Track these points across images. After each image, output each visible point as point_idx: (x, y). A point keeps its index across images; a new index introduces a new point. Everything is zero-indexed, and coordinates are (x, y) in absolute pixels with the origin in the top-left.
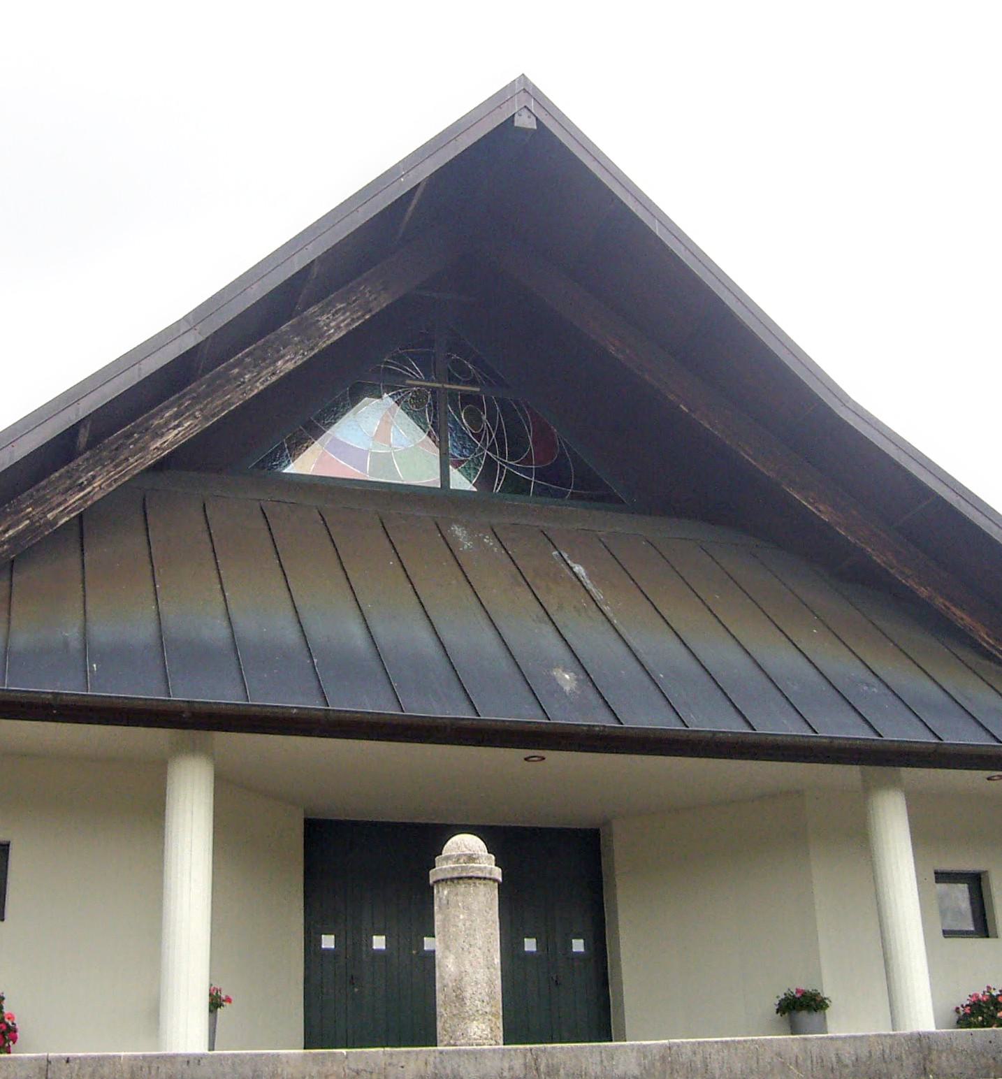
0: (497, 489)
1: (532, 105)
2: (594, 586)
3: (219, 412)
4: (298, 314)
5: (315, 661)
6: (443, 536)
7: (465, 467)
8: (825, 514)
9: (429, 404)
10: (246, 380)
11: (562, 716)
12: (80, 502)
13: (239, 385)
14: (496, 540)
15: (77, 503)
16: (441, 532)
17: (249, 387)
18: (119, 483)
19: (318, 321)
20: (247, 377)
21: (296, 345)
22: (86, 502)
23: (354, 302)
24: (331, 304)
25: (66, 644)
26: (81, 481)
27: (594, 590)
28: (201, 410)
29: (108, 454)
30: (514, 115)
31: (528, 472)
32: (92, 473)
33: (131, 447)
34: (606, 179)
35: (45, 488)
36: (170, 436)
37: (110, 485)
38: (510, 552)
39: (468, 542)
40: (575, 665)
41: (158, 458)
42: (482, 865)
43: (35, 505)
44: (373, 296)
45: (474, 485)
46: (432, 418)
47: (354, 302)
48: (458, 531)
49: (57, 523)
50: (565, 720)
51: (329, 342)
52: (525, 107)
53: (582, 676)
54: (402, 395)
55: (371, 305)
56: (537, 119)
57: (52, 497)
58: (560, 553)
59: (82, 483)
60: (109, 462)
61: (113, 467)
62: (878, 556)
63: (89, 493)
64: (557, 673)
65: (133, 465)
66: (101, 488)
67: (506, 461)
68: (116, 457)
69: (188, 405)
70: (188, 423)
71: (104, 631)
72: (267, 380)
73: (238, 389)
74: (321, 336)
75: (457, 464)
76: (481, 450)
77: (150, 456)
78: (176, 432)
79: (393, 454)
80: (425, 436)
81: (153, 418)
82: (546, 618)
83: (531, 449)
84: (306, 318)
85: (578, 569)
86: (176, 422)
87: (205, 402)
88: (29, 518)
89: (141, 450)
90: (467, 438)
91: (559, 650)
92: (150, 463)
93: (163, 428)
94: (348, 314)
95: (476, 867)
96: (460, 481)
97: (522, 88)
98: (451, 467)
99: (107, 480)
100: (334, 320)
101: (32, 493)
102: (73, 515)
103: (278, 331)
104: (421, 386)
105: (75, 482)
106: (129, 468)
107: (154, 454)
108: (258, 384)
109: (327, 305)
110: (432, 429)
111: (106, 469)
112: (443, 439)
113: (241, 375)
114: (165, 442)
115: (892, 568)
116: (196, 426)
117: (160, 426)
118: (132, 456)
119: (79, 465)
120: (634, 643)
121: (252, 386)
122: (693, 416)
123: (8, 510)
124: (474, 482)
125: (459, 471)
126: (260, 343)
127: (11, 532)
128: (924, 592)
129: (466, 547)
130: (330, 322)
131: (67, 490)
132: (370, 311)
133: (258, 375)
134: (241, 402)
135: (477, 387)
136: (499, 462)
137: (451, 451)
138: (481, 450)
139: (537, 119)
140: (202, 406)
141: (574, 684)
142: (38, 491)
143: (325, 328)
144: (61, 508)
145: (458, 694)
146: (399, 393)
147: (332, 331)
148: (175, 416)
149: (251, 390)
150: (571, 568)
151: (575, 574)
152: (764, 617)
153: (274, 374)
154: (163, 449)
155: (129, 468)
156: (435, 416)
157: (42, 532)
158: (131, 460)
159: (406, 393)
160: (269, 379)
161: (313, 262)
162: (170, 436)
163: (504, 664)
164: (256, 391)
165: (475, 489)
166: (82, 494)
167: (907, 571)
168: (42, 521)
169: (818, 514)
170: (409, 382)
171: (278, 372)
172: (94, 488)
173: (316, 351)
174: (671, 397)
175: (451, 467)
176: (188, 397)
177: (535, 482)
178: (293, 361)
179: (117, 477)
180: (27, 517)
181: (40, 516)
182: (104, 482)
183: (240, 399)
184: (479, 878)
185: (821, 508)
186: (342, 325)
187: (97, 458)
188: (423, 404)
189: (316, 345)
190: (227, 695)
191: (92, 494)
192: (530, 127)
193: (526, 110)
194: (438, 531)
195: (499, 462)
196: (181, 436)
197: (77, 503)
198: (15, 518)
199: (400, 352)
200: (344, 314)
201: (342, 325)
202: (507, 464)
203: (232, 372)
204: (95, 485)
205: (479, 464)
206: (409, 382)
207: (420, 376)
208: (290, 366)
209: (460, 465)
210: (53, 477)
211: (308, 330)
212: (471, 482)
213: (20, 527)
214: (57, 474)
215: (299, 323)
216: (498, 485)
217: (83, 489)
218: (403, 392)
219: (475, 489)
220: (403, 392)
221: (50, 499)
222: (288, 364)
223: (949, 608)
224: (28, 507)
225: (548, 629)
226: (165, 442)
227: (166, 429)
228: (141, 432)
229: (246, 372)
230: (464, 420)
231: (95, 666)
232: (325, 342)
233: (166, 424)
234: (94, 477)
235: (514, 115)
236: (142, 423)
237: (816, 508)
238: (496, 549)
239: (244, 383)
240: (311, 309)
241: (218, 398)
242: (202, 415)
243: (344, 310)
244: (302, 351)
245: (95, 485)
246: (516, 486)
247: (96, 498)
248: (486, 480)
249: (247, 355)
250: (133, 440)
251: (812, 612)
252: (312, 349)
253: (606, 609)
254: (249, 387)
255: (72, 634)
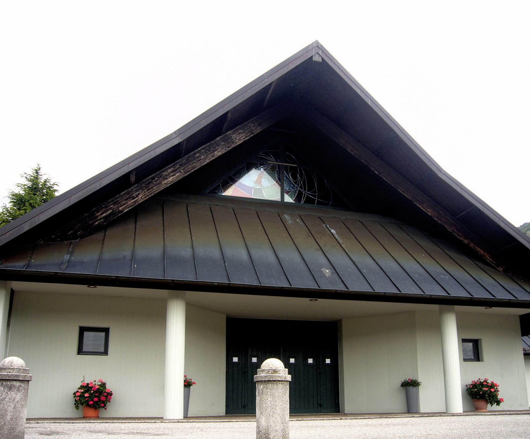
0: (302, 202)
1: (320, 52)
2: (339, 238)
3: (190, 171)
4: (223, 134)
5: (226, 264)
6: (281, 218)
7: (290, 194)
8: (429, 212)
9: (277, 171)
10: (202, 158)
11: (325, 286)
12: (133, 203)
13: (199, 160)
14: (301, 220)
15: (132, 204)
16: (280, 217)
17: (203, 161)
18: (149, 197)
19: (232, 137)
20: (202, 157)
21: (223, 146)
22: (135, 203)
23: (246, 130)
24: (237, 130)
25: (125, 257)
26: (133, 196)
27: (339, 239)
28: (183, 169)
29: (144, 185)
30: (312, 56)
31: (315, 196)
32: (137, 193)
33: (154, 183)
34: (349, 83)
35: (118, 198)
36: (171, 179)
37: (146, 197)
38: (306, 225)
39: (291, 221)
40: (330, 267)
41: (166, 187)
42: (281, 375)
43: (115, 204)
44: (254, 128)
45: (294, 200)
46: (278, 176)
47: (246, 130)
48: (287, 217)
49: (123, 212)
50: (326, 288)
51: (236, 145)
52: (317, 53)
53: (333, 271)
54: (267, 167)
55: (253, 131)
56: (322, 58)
57: (121, 202)
58: (326, 225)
59: (134, 196)
60: (145, 188)
61: (147, 190)
62: (449, 228)
63: (137, 200)
64: (323, 270)
65: (155, 190)
66: (142, 198)
67: (306, 192)
68: (148, 187)
69: (178, 167)
70: (178, 174)
71: (141, 253)
72: (210, 158)
73: (199, 162)
74: (233, 143)
75: (287, 193)
76: (297, 188)
77: (162, 187)
78: (173, 177)
79: (262, 189)
80: (275, 182)
81: (163, 172)
82: (320, 249)
83: (316, 189)
84: (227, 136)
85: (333, 231)
86: (173, 174)
87: (185, 166)
88: (111, 209)
89: (159, 184)
90: (291, 183)
91: (323, 260)
92: (162, 189)
93: (167, 176)
94: (244, 134)
95: (278, 376)
96: (288, 199)
97: (316, 45)
98: (285, 194)
99: (144, 195)
100: (239, 136)
101: (113, 200)
102: (130, 208)
103: (215, 140)
104: (274, 164)
105: (131, 195)
106: (153, 191)
107: (163, 186)
108: (207, 160)
109: (235, 131)
110: (278, 180)
111: (143, 191)
112: (282, 183)
113: (199, 157)
114: (168, 181)
115: (454, 233)
116: (181, 175)
117: (166, 175)
118: (155, 187)
119: (132, 189)
120: (354, 259)
121: (205, 160)
122: (380, 175)
123: (103, 206)
124: (294, 199)
125: (288, 195)
126: (208, 144)
127: (104, 215)
128: (466, 242)
129: (289, 223)
130: (237, 137)
131: (127, 199)
132: (253, 134)
133: (206, 157)
134: (200, 167)
135: (295, 164)
136: (303, 192)
137: (285, 188)
138: (297, 188)
139: (322, 58)
140: (184, 168)
141: (330, 274)
142: (115, 199)
143: (235, 140)
144: (125, 206)
145: (283, 277)
146: (265, 166)
147: (237, 141)
148: (173, 172)
149: (204, 162)
150: (330, 231)
151: (331, 233)
152: (405, 250)
153: (213, 156)
154: (167, 184)
155: (153, 191)
156: (279, 175)
157: (118, 215)
158: (154, 188)
159: (268, 166)
160: (211, 158)
161: (228, 111)
162: (171, 179)
163: (303, 266)
164: (206, 163)
165: (294, 202)
166: (134, 200)
167: (460, 234)
168: (117, 211)
169: (427, 212)
170: (269, 162)
171: (215, 155)
172: (139, 198)
173: (231, 148)
174: (372, 169)
175: (285, 194)
176: (178, 164)
177: (317, 200)
178: (221, 152)
179: (148, 194)
180: (111, 209)
181: (117, 209)
182: (143, 196)
183: (199, 166)
184: (279, 381)
185: (428, 210)
186: (241, 138)
187: (140, 187)
188: (275, 171)
189: (231, 146)
190: (189, 277)
191: (138, 200)
192: (319, 61)
193: (317, 54)
194: (279, 217)
195: (303, 192)
196: (175, 179)
197: (132, 204)
198: (106, 209)
199: (266, 151)
200: (242, 134)
201: (241, 138)
202: (306, 193)
203: (196, 155)
204: (139, 197)
205: (296, 193)
206: (269, 162)
207: (274, 160)
208: (220, 154)
209: (288, 193)
210: (121, 194)
211: (228, 140)
212: (292, 199)
213: (108, 213)
214: (123, 193)
215: (224, 137)
216: (303, 200)
217: (134, 198)
218: (267, 166)
219: (294, 202)
220: (267, 166)
221: (120, 202)
222: (219, 153)
223: (475, 248)
224: (111, 205)
225: (320, 253)
226: (168, 181)
227: (169, 176)
228: (158, 177)
229: (202, 155)
230: (290, 177)
231: (135, 265)
232: (234, 145)
233: (169, 174)
234: (139, 194)
235: (312, 56)
236: (158, 174)
237: (426, 210)
238: (301, 224)
239: (201, 159)
240: (228, 132)
241: (190, 165)
242: (184, 171)
243: (243, 133)
244: (225, 148)
245: (139, 197)
246: (309, 201)
247: (140, 202)
248: (298, 198)
249: (202, 149)
250: (155, 180)
251: (423, 248)
252: (229, 147)
253: (343, 246)
254: (203, 161)
255: (127, 253)
